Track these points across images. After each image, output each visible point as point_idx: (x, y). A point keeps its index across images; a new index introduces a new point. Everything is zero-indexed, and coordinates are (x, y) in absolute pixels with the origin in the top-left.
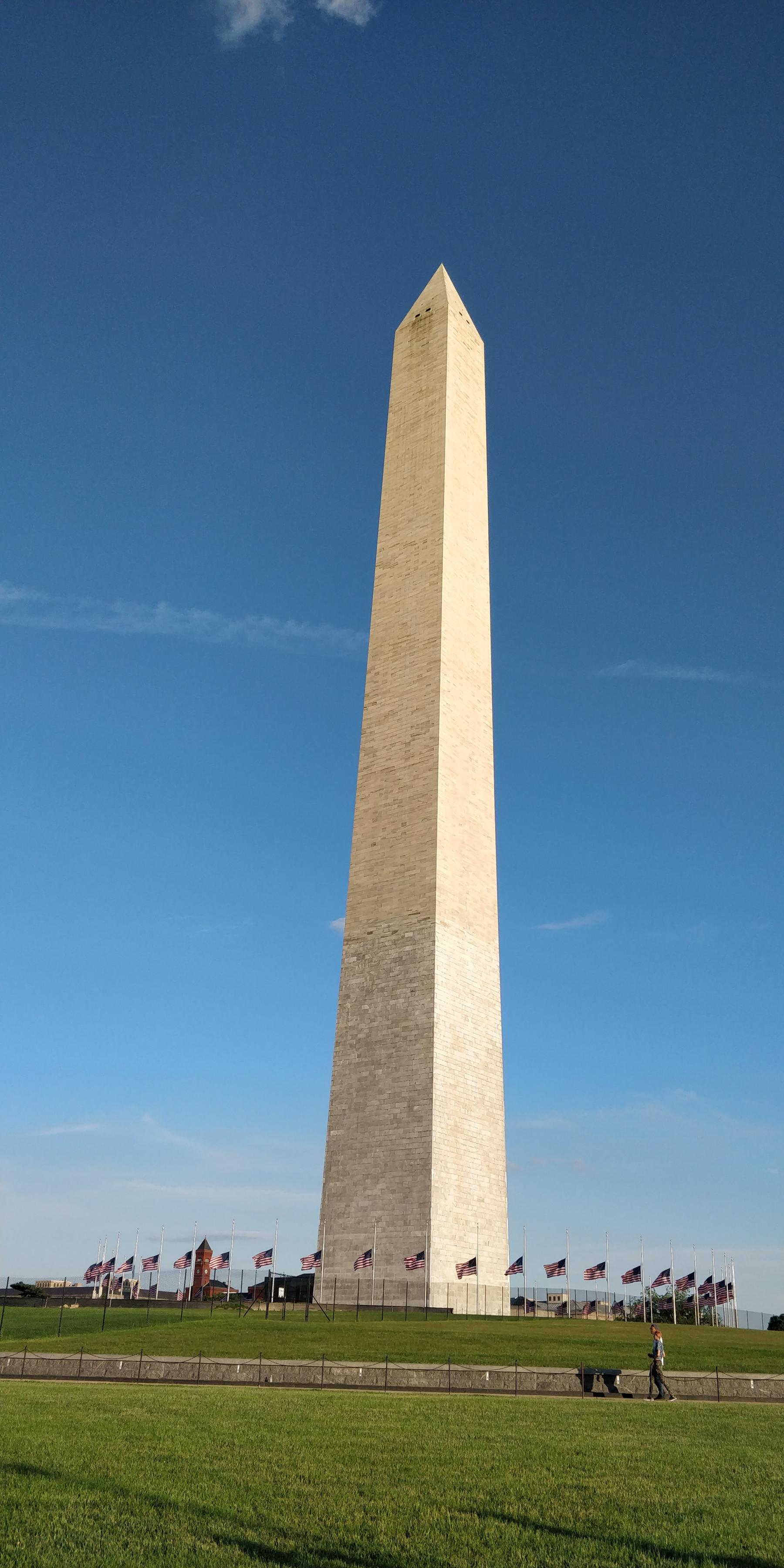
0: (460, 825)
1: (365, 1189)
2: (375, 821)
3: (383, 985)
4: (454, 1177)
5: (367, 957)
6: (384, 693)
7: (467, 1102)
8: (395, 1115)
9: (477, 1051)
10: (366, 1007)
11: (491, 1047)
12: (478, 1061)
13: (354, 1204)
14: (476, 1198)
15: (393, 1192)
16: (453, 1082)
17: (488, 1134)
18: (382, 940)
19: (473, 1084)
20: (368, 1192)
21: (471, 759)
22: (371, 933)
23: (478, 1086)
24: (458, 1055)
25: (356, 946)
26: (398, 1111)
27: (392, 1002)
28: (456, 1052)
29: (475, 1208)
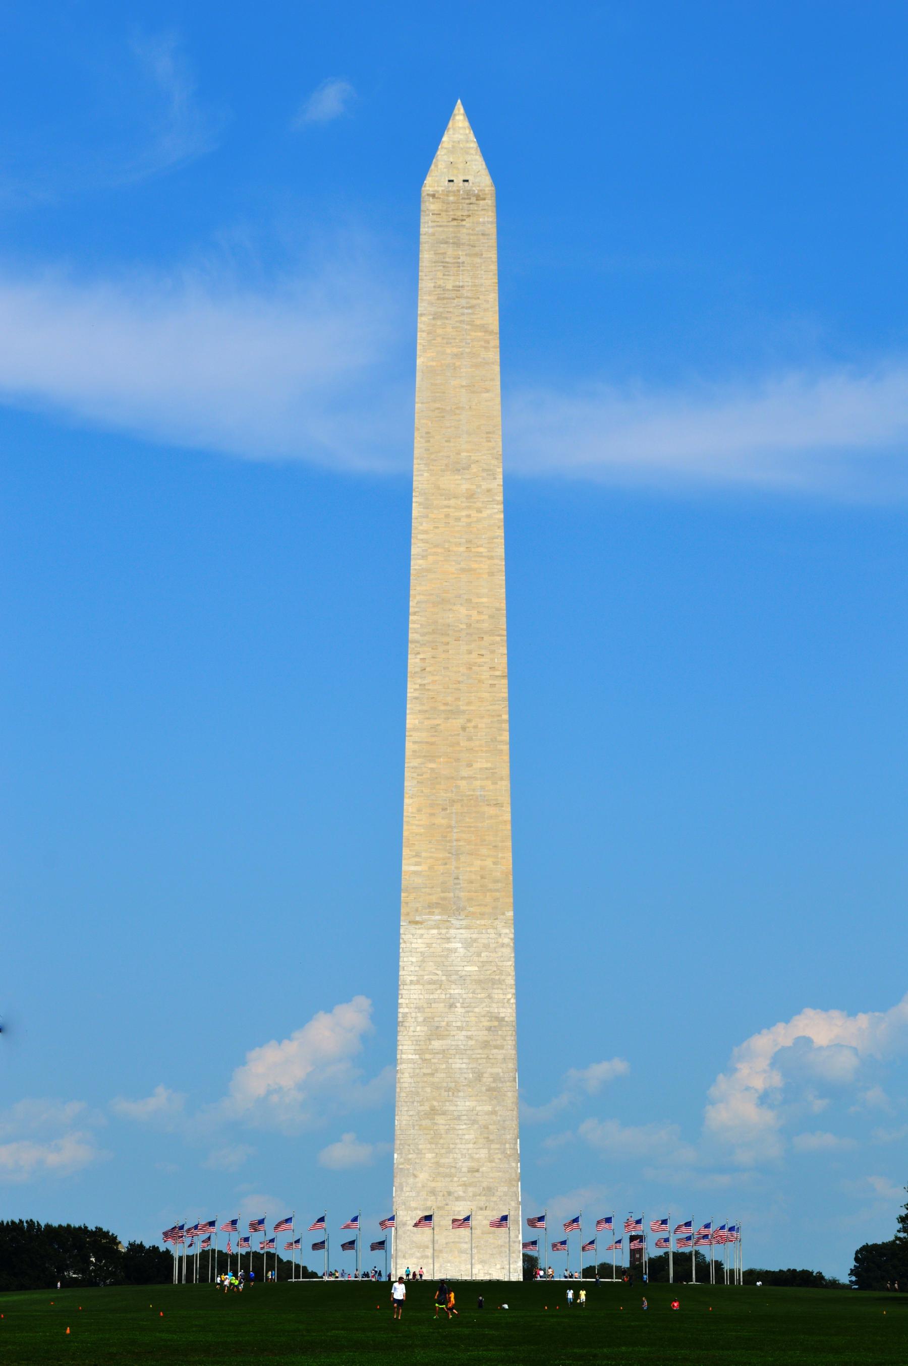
0: (444, 809)
4: (429, 1156)
7: (452, 1085)
9: (469, 1033)
11: (496, 1023)
12: (471, 1043)
14: (465, 1170)
16: (429, 1071)
17: (489, 1108)
19: (464, 1066)
21: (464, 729)
23: (470, 1066)
24: (436, 1044)
28: (433, 1042)
29: (465, 1179)
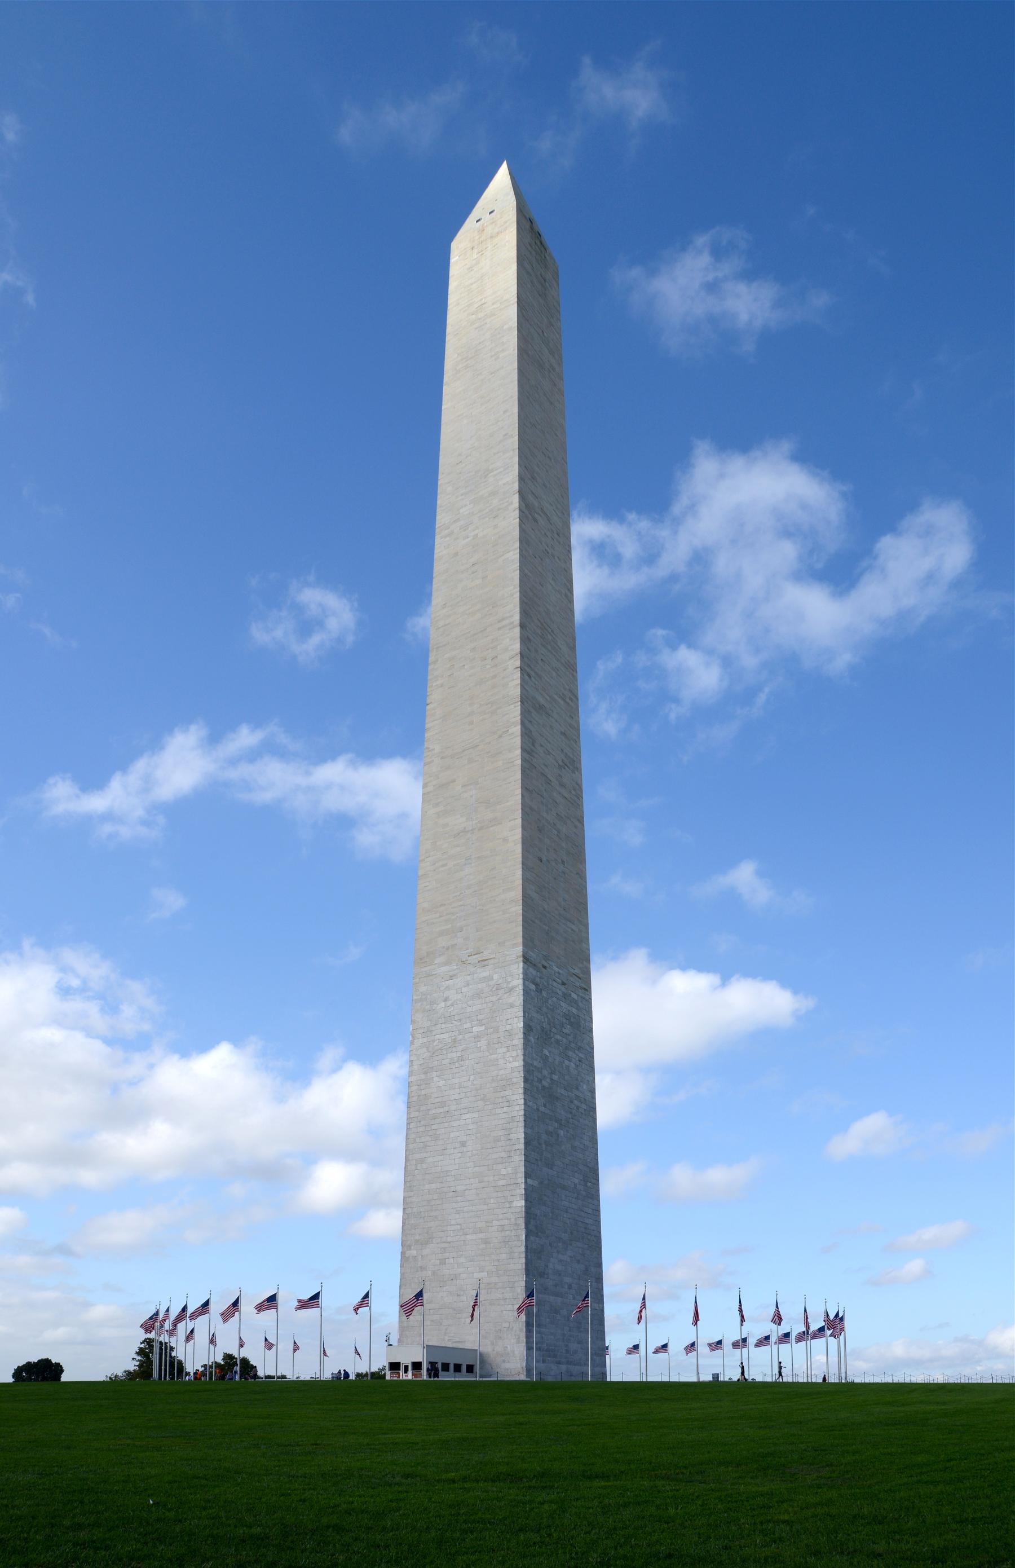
1: (558, 1252)
2: (540, 831)
3: (558, 1037)
5: (544, 994)
6: (537, 674)
8: (575, 1185)
10: (546, 1052)
13: (551, 1265)
15: (578, 1262)
18: (555, 984)
20: (561, 1257)
22: (545, 967)
25: (534, 972)
26: (576, 1181)
27: (567, 1062)
